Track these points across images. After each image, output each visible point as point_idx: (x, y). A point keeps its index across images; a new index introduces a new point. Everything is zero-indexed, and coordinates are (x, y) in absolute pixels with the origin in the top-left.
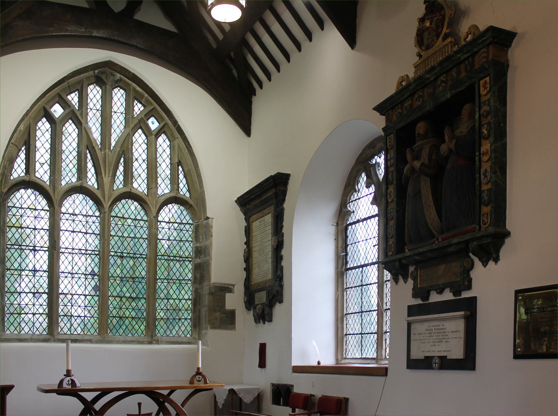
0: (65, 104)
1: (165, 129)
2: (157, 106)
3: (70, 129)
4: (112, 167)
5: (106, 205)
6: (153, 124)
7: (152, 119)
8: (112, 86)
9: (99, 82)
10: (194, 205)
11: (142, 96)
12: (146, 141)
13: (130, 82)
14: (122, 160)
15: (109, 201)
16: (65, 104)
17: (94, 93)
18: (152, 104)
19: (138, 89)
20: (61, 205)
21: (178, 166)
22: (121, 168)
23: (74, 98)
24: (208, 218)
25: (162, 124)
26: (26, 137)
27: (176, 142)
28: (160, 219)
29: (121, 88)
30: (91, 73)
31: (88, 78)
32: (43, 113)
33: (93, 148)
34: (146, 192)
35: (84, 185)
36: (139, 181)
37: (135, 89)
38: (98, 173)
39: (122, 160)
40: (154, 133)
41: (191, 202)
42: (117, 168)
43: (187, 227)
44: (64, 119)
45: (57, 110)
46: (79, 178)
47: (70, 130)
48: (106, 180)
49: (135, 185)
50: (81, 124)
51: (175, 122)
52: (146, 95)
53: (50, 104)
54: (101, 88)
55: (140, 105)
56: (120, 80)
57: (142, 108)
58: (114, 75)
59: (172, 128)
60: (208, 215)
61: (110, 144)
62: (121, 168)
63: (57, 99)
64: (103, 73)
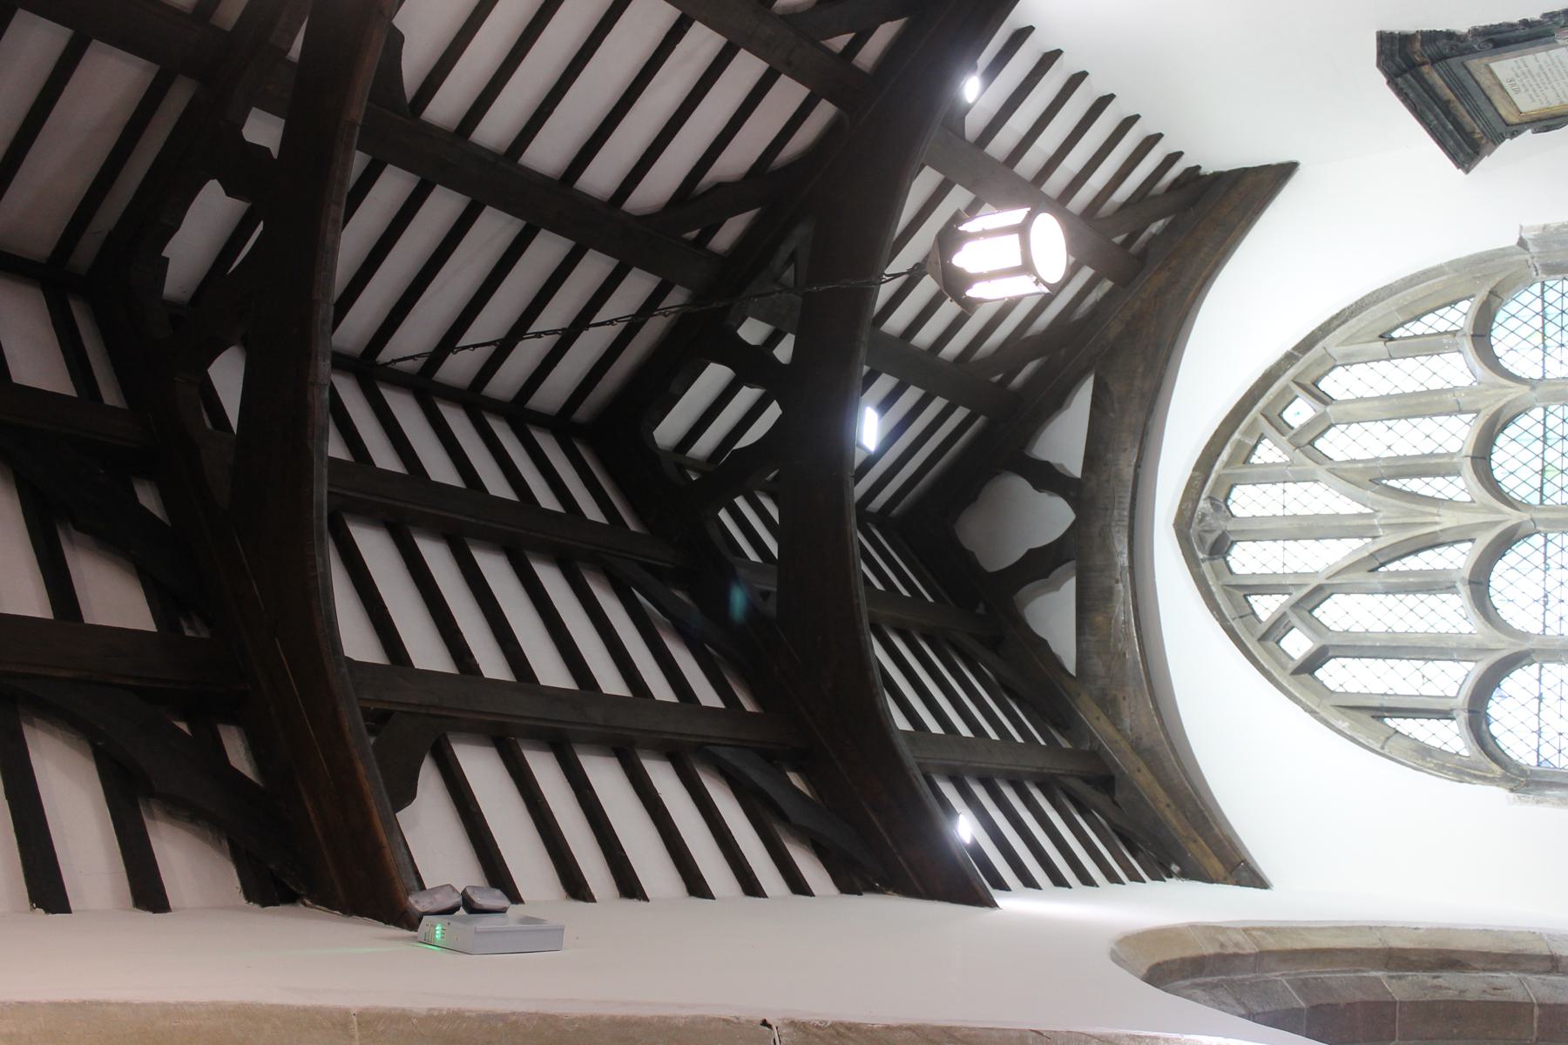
0: (1279, 627)
1: (1308, 382)
2: (1254, 408)
3: (1339, 613)
4: (1414, 506)
5: (1512, 517)
6: (1300, 412)
7: (1288, 415)
8: (1227, 519)
9: (1220, 548)
10: (1487, 287)
11: (1240, 444)
12: (1342, 427)
13: (1213, 476)
14: (1393, 483)
15: (1499, 512)
16: (1279, 627)
17: (1246, 559)
18: (1255, 420)
19: (1224, 456)
20: (1525, 635)
21: (1392, 339)
22: (1414, 485)
23: (1266, 607)
24: (1522, 243)
25: (1297, 390)
26: (1365, 717)
27: (1336, 351)
28: (1537, 375)
29: (1227, 497)
30: (1205, 567)
31: (1217, 575)
32: (1306, 676)
33: (1372, 555)
34: (1468, 417)
35: (1467, 575)
36: (1440, 436)
37: (1227, 464)
38: (1432, 543)
39: (1393, 483)
40: (1320, 408)
41: (1482, 294)
42: (1413, 497)
43: (1550, 296)
44: (1316, 628)
45: (1297, 644)
46: (1450, 588)
47: (1339, 613)
48: (1447, 520)
49: (1453, 446)
50: (1319, 588)
51: (1290, 358)
52: (1236, 436)
53: (1284, 659)
54: (1233, 543)
55: (1261, 449)
56: (1211, 498)
57: (1266, 442)
58: (1204, 515)
59: (1300, 367)
60: (1513, 242)
61: (1360, 515)
62: (1414, 485)
63: (1271, 644)
64: (1202, 540)
